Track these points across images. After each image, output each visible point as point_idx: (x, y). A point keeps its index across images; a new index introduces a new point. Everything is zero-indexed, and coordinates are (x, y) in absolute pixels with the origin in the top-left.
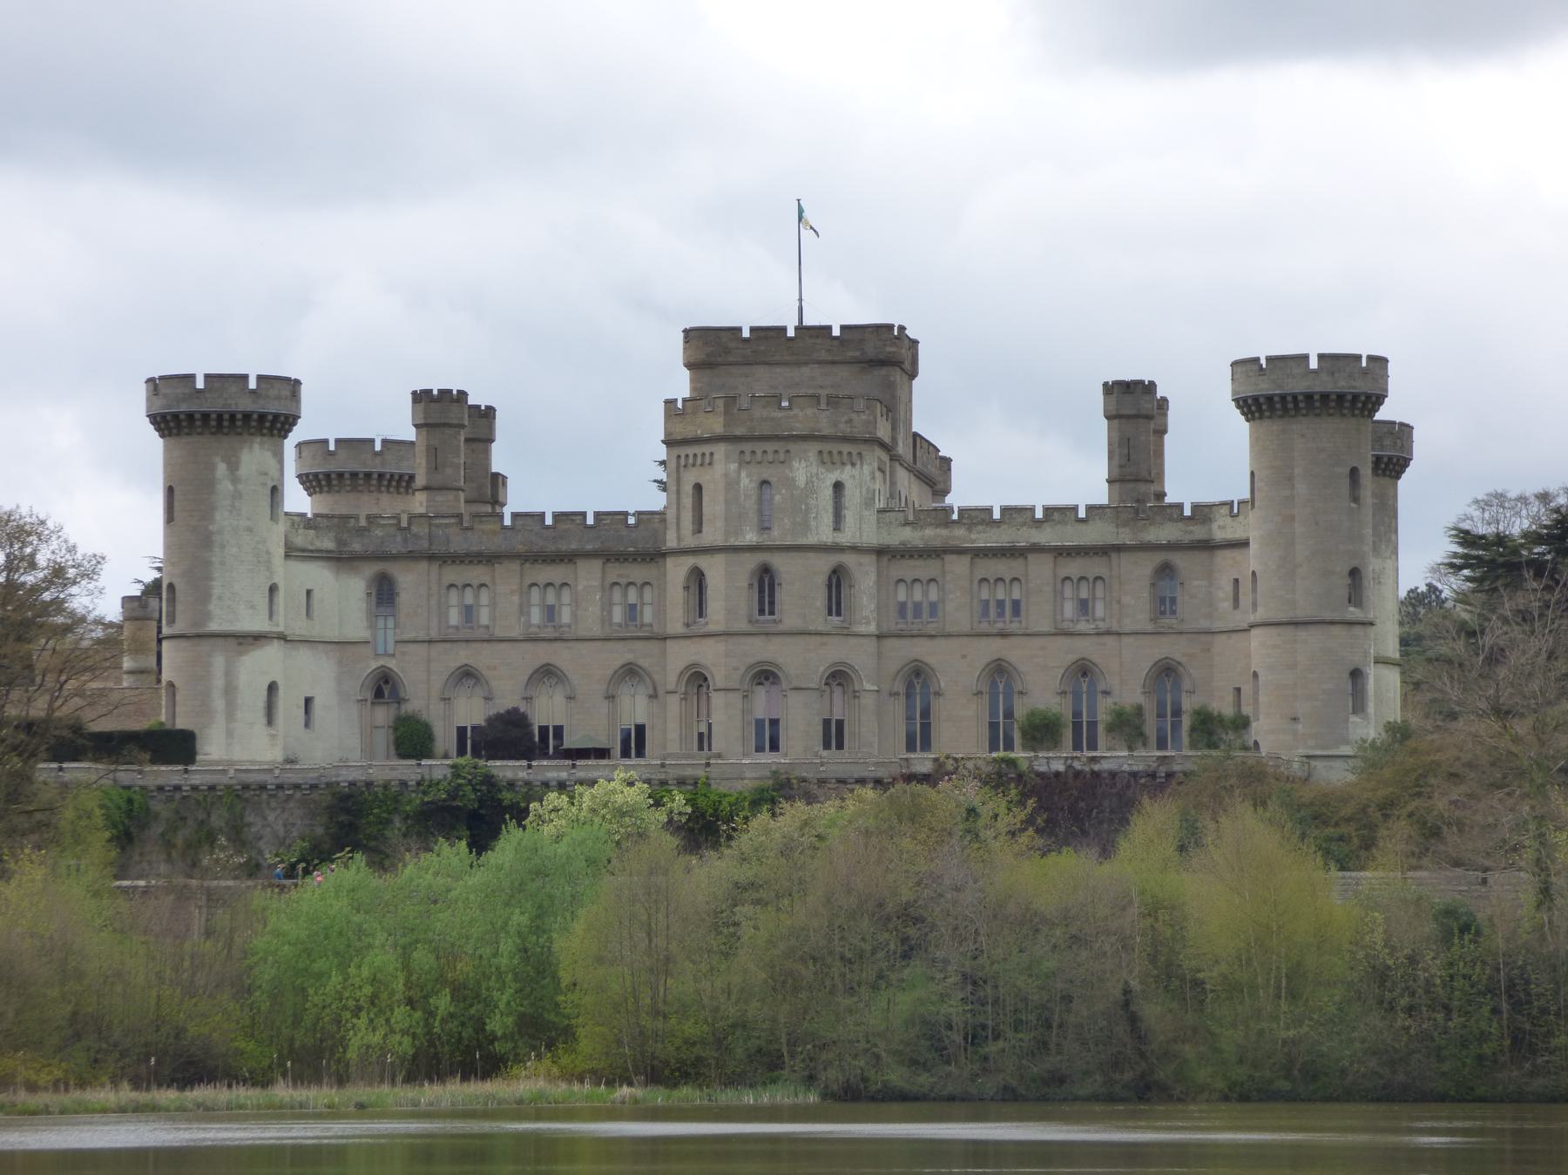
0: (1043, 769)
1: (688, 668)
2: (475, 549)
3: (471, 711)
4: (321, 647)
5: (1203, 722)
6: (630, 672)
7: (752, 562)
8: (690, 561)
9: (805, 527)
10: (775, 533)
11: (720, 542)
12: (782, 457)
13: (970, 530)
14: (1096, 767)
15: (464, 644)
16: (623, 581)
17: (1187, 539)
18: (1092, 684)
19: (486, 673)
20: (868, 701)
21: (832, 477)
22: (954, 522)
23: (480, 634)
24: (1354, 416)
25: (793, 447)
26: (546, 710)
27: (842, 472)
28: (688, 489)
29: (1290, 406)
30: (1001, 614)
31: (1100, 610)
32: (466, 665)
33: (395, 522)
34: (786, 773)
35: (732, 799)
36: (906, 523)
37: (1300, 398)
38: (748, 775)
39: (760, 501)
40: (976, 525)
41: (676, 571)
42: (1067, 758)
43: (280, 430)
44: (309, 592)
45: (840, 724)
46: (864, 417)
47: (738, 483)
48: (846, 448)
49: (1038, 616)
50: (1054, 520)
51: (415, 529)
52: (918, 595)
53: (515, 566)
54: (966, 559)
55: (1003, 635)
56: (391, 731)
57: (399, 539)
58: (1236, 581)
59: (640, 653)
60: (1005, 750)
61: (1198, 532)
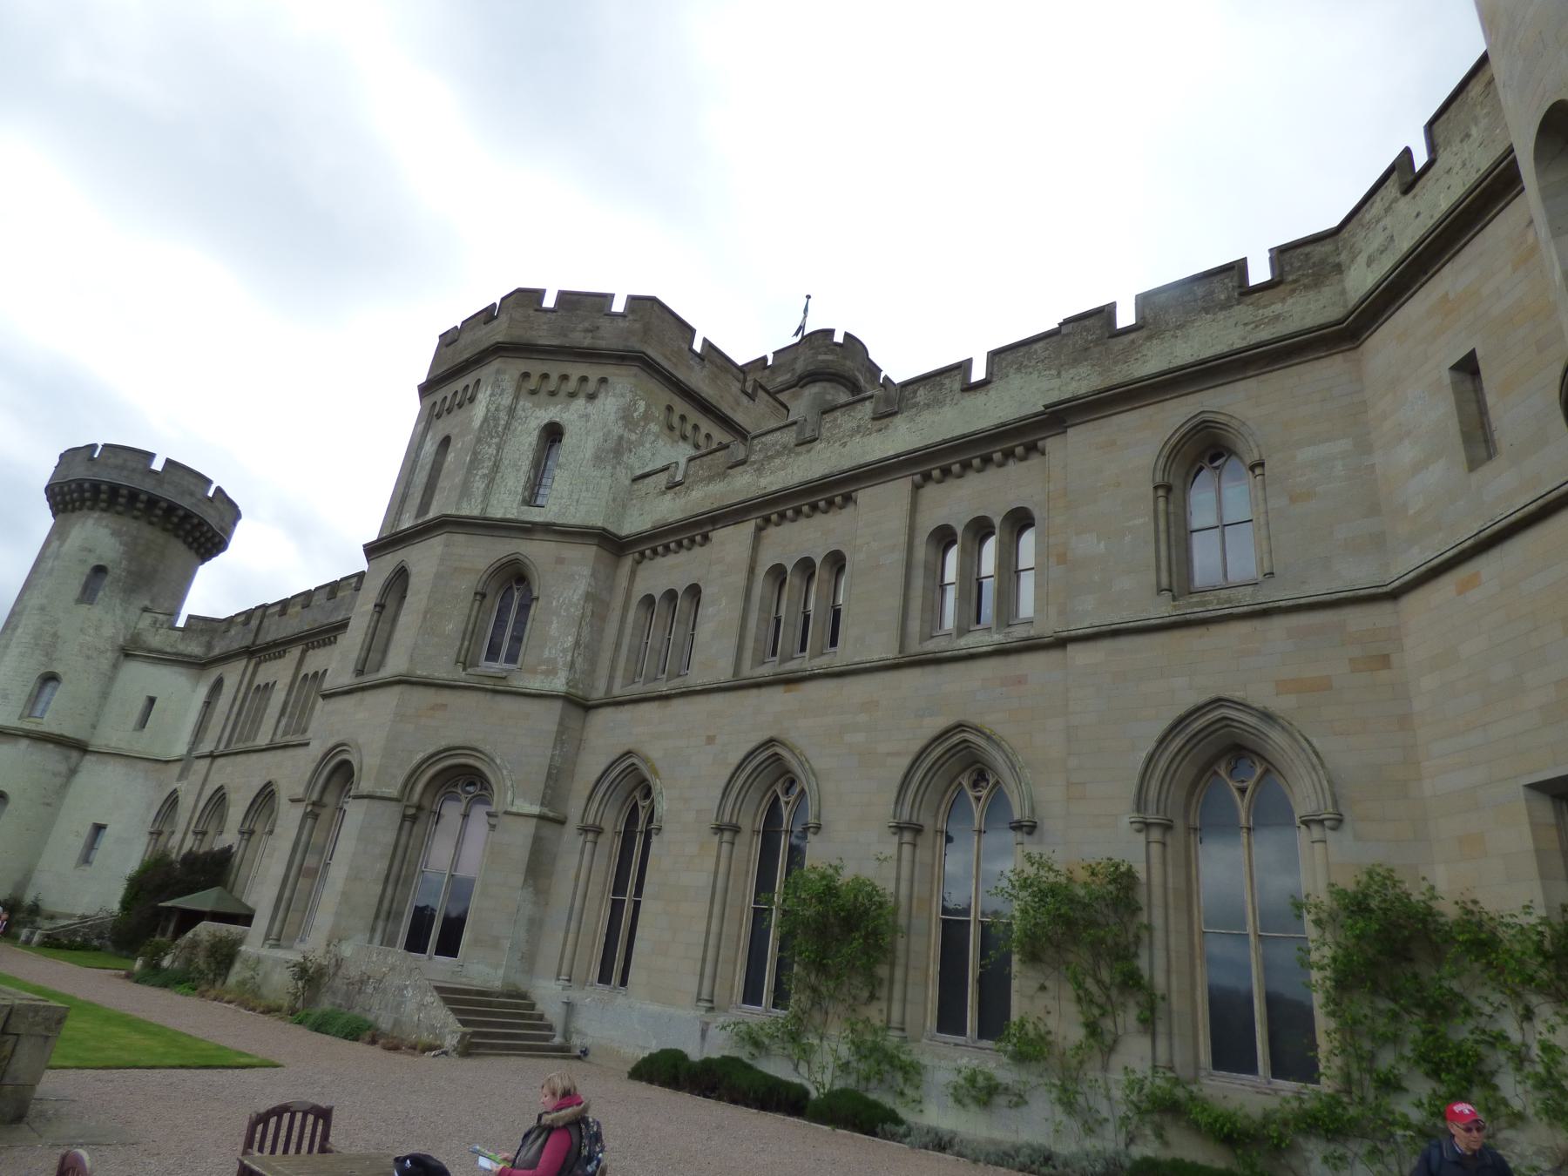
4: (141, 765)
44: (152, 701)
46: (622, 324)
48: (576, 370)
50: (916, 405)
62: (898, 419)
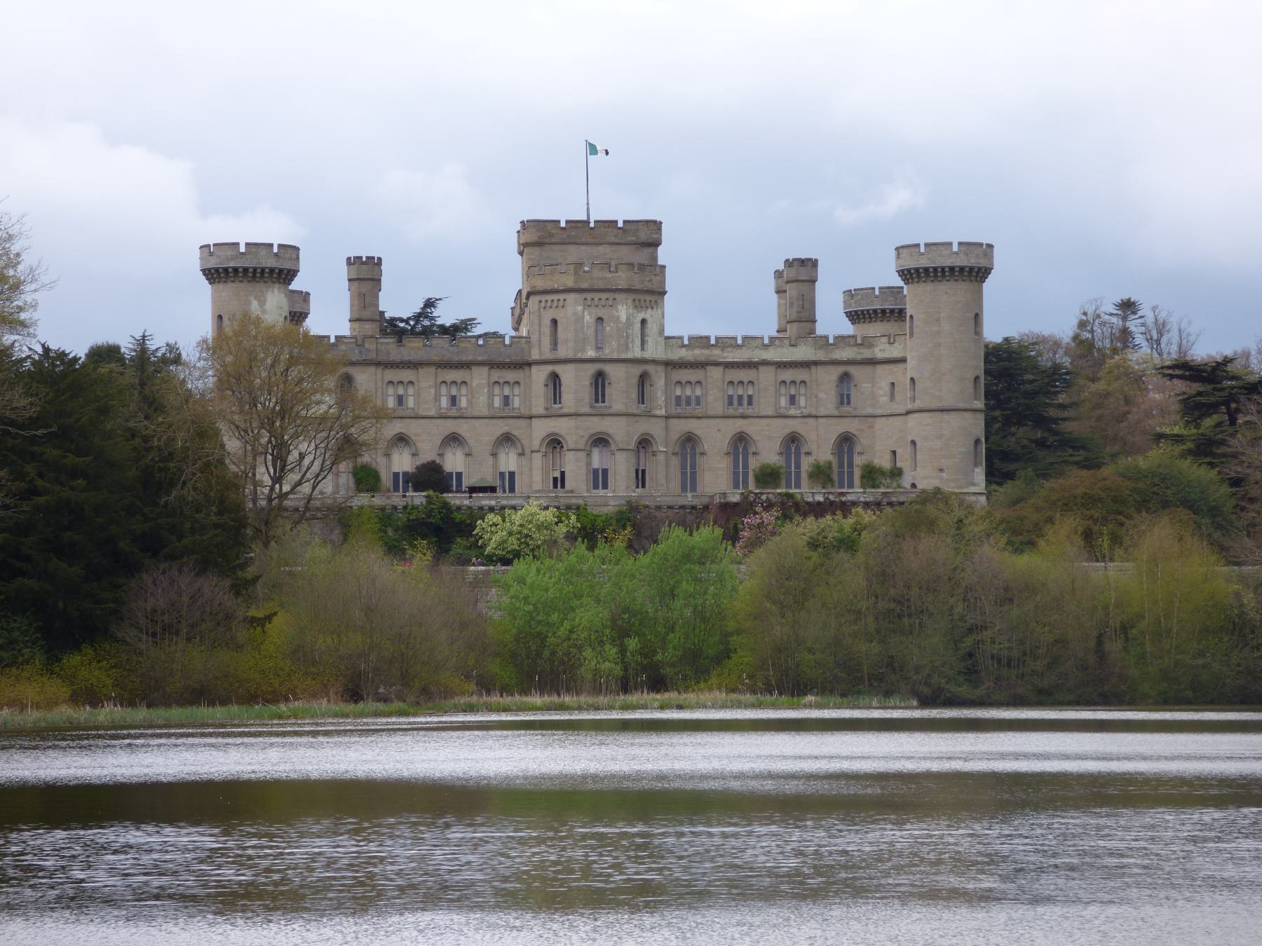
0: (810, 500)
1: (548, 436)
2: (406, 358)
3: (403, 462)
5: (870, 472)
6: (507, 439)
7: (592, 369)
8: (550, 368)
9: (627, 349)
10: (607, 351)
11: (571, 355)
12: (610, 302)
13: (723, 350)
14: (844, 499)
15: (399, 420)
16: (501, 381)
17: (859, 357)
18: (798, 449)
19: (412, 438)
20: (661, 457)
21: (641, 316)
22: (713, 345)
23: (408, 413)
24: (977, 281)
25: (618, 296)
26: (453, 462)
27: (646, 313)
28: (547, 322)
29: (939, 274)
30: (740, 404)
31: (802, 401)
32: (401, 433)
33: (353, 340)
34: (636, 502)
35: (603, 518)
36: (683, 346)
37: (947, 269)
38: (612, 503)
39: (596, 331)
40: (727, 347)
41: (539, 375)
42: (825, 493)
43: (284, 279)
45: (644, 471)
47: (583, 318)
48: (648, 298)
49: (765, 405)
51: (367, 345)
52: (688, 392)
53: (432, 370)
54: (721, 369)
55: (744, 417)
56: (351, 476)
57: (357, 351)
58: (893, 384)
59: (516, 428)
60: (796, 488)
61: (866, 353)
62: (770, 348)
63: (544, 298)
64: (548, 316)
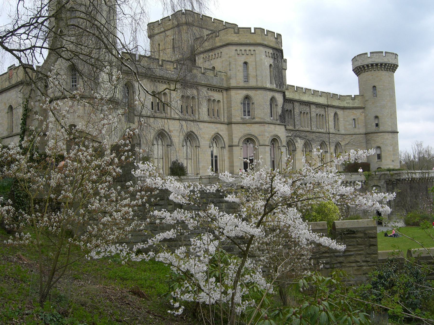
1: (244, 136)
8: (245, 93)
63: (239, 48)
64: (242, 59)
